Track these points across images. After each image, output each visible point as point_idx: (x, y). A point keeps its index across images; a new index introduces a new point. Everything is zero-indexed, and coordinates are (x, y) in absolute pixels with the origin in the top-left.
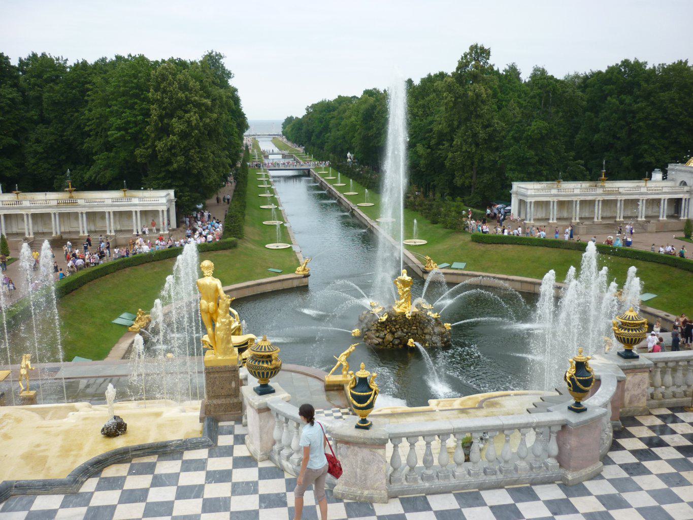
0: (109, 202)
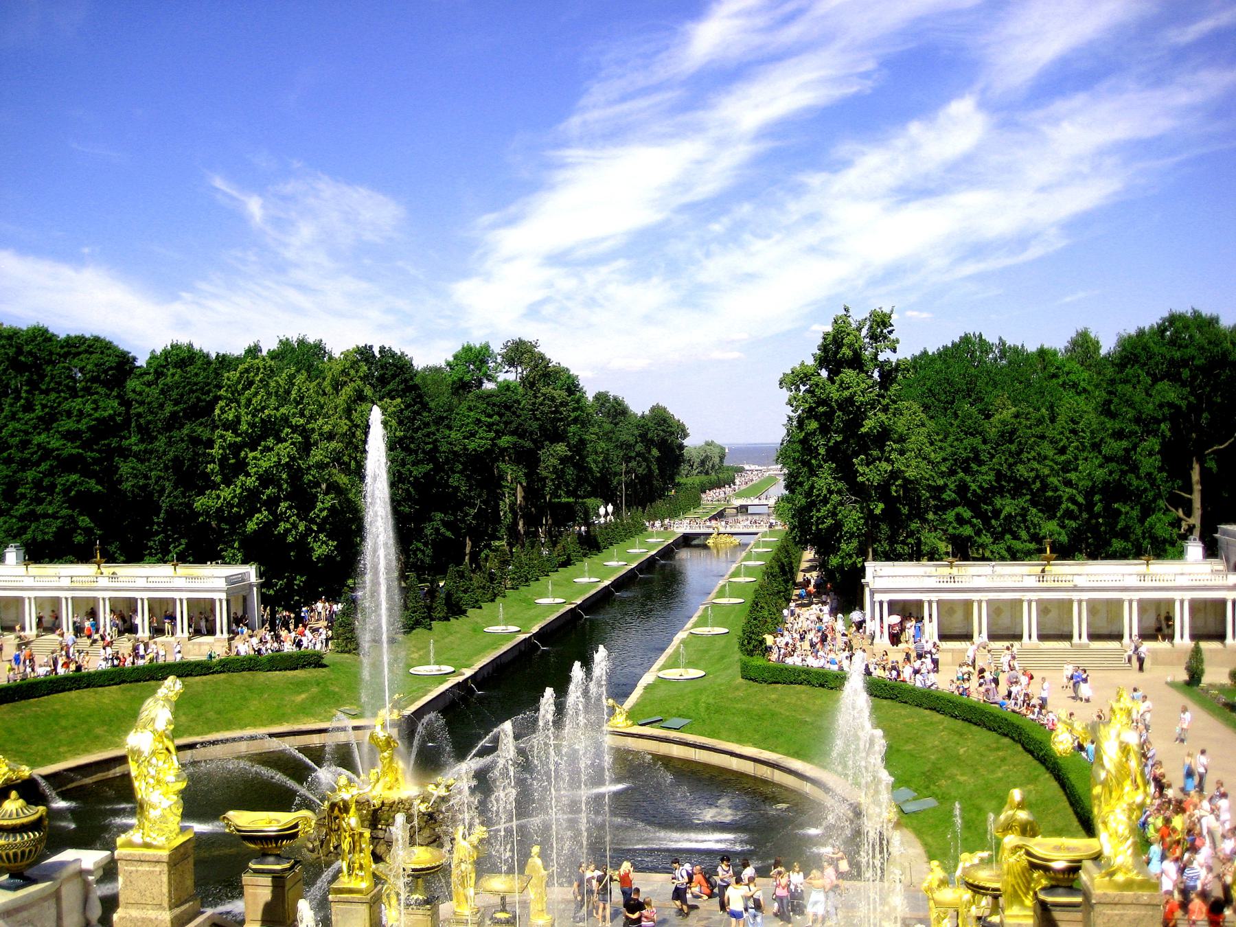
0: (141, 583)
